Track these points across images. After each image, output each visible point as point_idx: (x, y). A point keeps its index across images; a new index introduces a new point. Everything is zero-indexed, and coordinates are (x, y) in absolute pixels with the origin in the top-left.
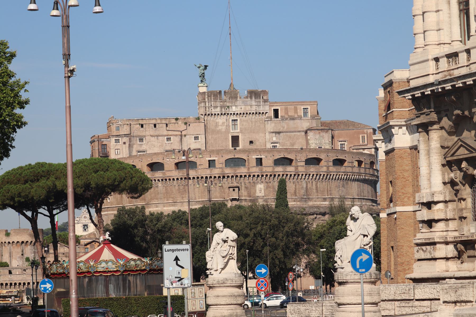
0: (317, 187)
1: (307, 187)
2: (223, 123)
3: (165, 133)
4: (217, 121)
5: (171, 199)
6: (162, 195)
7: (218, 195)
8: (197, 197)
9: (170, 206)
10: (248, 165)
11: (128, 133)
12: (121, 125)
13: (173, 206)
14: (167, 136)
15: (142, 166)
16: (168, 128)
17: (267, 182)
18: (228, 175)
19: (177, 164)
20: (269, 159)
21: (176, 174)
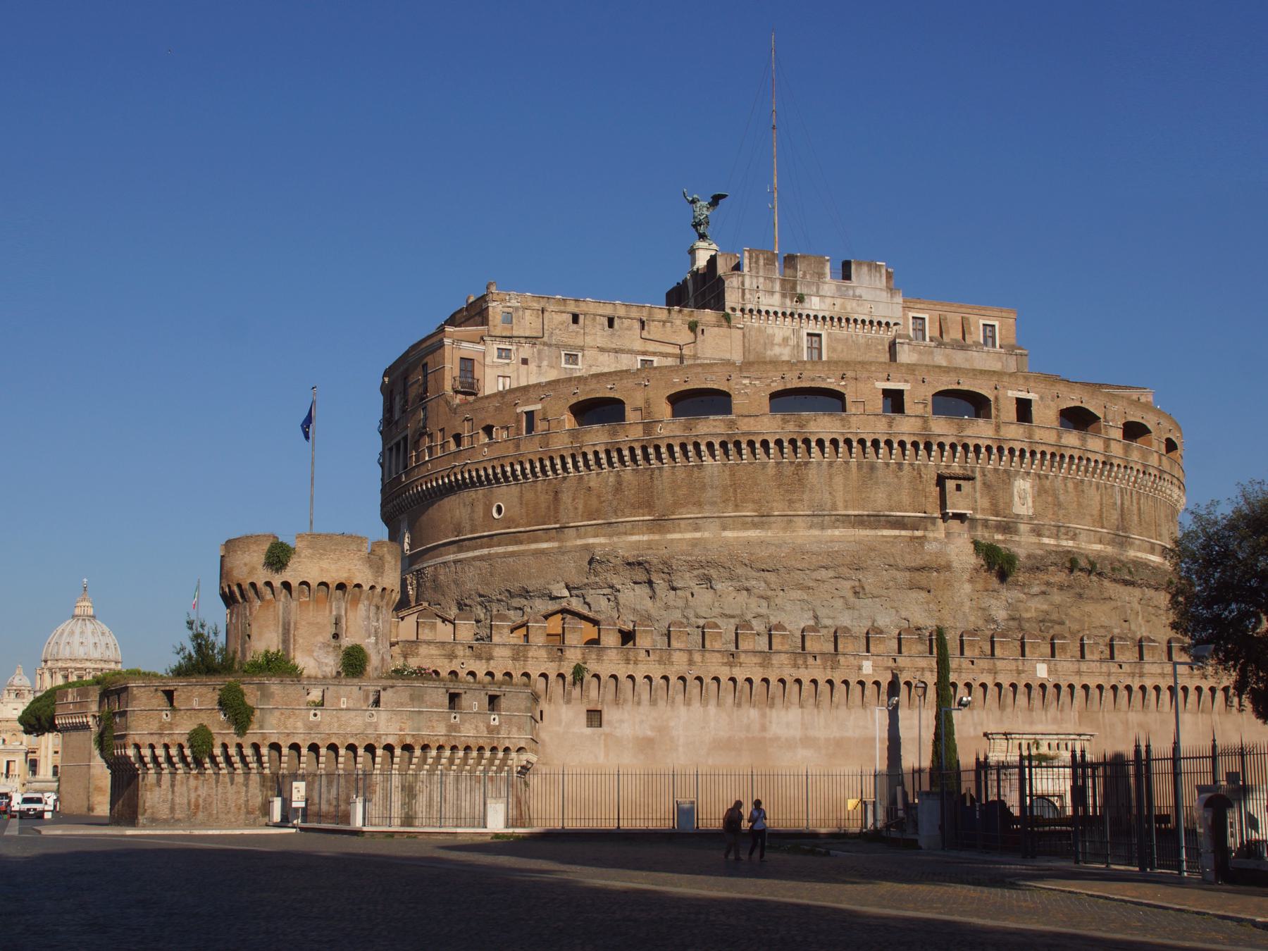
0: (1139, 509)
1: (1122, 504)
2: (785, 340)
3: (638, 345)
4: (769, 331)
5: (751, 506)
6: (718, 493)
7: (906, 499)
8: (840, 504)
9: (744, 526)
10: (997, 416)
11: (535, 335)
12: (517, 309)
13: (755, 526)
14: (644, 353)
15: (647, 401)
16: (645, 334)
17: (1039, 476)
18: (941, 439)
19: (774, 396)
20: (1048, 407)
21: (770, 426)
